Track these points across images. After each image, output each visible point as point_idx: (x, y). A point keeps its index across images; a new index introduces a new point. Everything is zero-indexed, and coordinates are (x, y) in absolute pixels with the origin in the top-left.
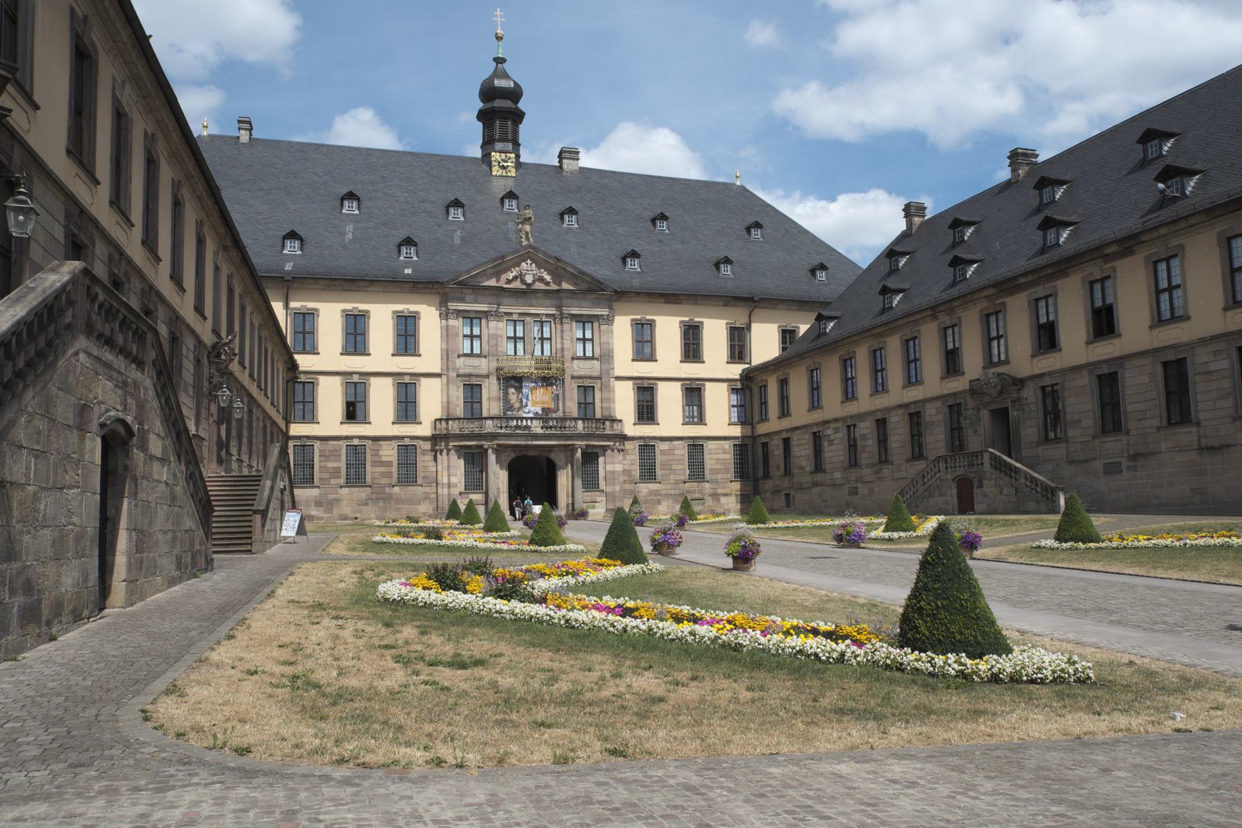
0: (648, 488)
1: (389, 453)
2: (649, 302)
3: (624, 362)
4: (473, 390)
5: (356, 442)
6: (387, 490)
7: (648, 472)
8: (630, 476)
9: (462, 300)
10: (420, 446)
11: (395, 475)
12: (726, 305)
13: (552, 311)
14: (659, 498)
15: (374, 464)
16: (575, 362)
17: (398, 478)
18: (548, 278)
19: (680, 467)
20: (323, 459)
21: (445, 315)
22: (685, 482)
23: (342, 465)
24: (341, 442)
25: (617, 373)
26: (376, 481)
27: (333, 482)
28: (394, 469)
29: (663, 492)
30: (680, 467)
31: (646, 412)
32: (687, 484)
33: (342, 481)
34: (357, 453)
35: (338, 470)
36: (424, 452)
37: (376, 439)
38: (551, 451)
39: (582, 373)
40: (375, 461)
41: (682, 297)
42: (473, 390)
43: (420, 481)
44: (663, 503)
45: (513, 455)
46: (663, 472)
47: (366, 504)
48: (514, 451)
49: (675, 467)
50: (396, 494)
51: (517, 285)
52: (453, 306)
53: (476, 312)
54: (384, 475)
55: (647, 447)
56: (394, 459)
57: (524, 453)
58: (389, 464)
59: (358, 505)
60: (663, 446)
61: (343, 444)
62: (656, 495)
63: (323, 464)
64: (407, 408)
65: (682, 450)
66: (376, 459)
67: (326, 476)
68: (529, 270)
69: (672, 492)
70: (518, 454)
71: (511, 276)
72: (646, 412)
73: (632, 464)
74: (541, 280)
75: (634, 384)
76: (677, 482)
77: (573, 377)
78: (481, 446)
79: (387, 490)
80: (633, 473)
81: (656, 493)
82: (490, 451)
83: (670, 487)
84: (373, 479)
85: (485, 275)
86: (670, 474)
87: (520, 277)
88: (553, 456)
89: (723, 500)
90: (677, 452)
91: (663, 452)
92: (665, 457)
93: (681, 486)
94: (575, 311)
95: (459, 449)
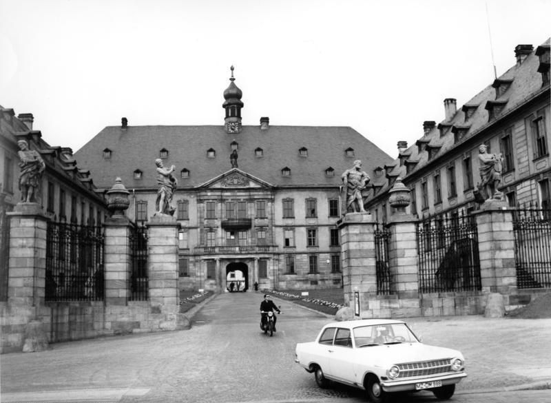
45: (228, 263)
77: (255, 226)
88: (246, 263)
89: (326, 282)
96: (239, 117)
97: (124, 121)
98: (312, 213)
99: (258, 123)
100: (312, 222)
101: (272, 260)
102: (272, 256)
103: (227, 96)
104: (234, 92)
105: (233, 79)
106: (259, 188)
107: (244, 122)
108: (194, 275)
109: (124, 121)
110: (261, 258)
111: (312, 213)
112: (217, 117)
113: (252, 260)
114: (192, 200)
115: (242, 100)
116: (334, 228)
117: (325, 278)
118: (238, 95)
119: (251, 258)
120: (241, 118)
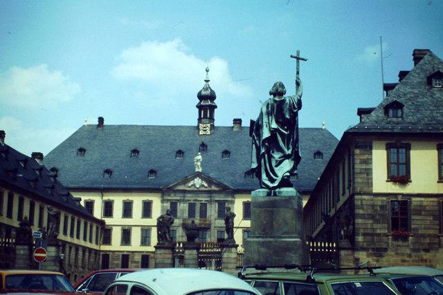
1: (138, 258)
5: (125, 253)
9: (169, 195)
13: (209, 199)
18: (206, 185)
21: (163, 201)
36: (152, 258)
37: (133, 252)
51: (192, 188)
52: (166, 198)
58: (138, 262)
68: (198, 182)
71: (190, 185)
74: (203, 186)
85: (179, 184)
87: (194, 185)
94: (216, 199)
96: (212, 119)
97: (101, 120)
99: (231, 124)
103: (201, 97)
104: (208, 92)
106: (220, 191)
107: (216, 124)
109: (101, 120)
112: (190, 117)
115: (216, 102)
118: (212, 97)
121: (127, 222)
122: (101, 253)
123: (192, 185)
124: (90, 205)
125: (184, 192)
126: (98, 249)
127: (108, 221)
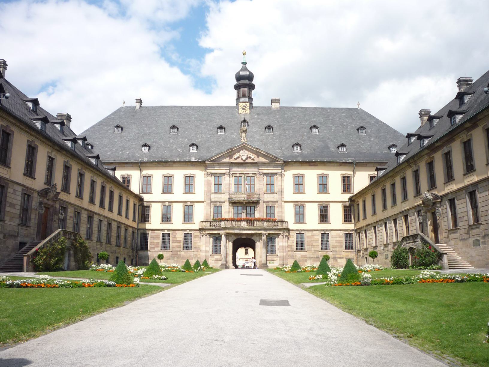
0: (300, 254)
1: (180, 236)
2: (302, 166)
3: (289, 194)
4: (218, 208)
5: (166, 232)
6: (179, 253)
7: (300, 246)
8: (292, 248)
10: (194, 234)
11: (182, 246)
12: (340, 166)
14: (306, 259)
15: (174, 241)
16: (265, 194)
17: (184, 248)
19: (317, 244)
20: (152, 239)
22: (319, 251)
23: (160, 241)
24: (160, 232)
25: (286, 200)
26: (174, 249)
27: (156, 249)
28: (182, 244)
29: (308, 256)
30: (317, 244)
31: (300, 217)
32: (320, 253)
33: (160, 248)
34: (166, 237)
35: (158, 244)
37: (175, 230)
38: (253, 236)
39: (269, 200)
40: (174, 240)
41: (317, 163)
42: (218, 208)
43: (193, 249)
44: (308, 262)
45: (235, 238)
46: (308, 246)
47: (170, 259)
48: (235, 236)
49: (314, 244)
50: (182, 255)
53: (220, 173)
54: (177, 246)
55: (300, 234)
56: (182, 240)
57: (240, 237)
58: (180, 241)
59: (166, 259)
60: (307, 234)
61: (161, 232)
62: (305, 257)
63: (152, 241)
64: (188, 217)
65: (318, 236)
66: (175, 239)
67: (153, 246)
69: (313, 256)
70: (237, 237)
72: (300, 217)
73: (292, 243)
75: (294, 204)
76: (315, 252)
78: (219, 234)
79: (179, 253)
80: (293, 247)
81: (304, 257)
82: (223, 236)
83: (311, 254)
84: (173, 248)
85: (223, 157)
86: (312, 248)
90: (315, 237)
91: (308, 237)
92: (309, 240)
93: (317, 253)
95: (211, 235)
96: (250, 99)
98: (323, 188)
100: (323, 197)
101: (281, 236)
102: (281, 232)
103: (239, 78)
104: (246, 73)
105: (244, 63)
106: (268, 163)
107: (254, 104)
108: (198, 250)
110: (269, 234)
111: (323, 188)
113: (260, 235)
114: (199, 174)
116: (348, 204)
117: (337, 256)
118: (250, 77)
119: (260, 234)
120: (252, 99)
121: (167, 197)
122: (140, 232)
123: (238, 157)
124: (127, 180)
125: (230, 164)
126: (136, 227)
127: (146, 197)
